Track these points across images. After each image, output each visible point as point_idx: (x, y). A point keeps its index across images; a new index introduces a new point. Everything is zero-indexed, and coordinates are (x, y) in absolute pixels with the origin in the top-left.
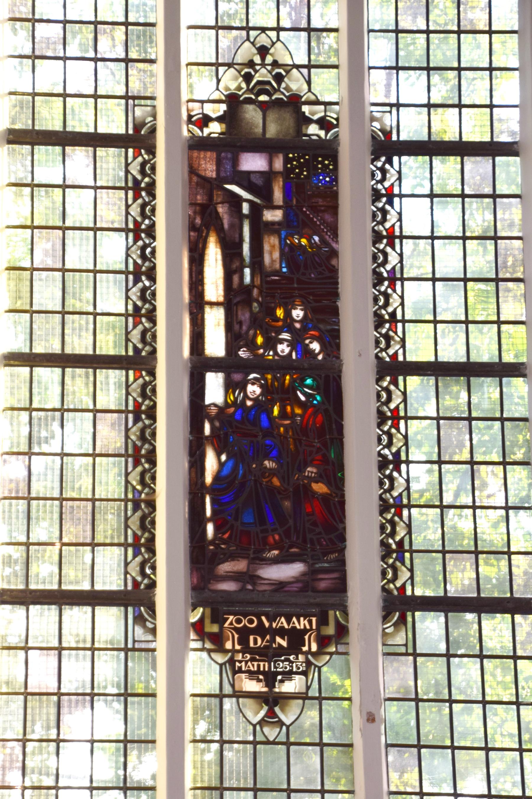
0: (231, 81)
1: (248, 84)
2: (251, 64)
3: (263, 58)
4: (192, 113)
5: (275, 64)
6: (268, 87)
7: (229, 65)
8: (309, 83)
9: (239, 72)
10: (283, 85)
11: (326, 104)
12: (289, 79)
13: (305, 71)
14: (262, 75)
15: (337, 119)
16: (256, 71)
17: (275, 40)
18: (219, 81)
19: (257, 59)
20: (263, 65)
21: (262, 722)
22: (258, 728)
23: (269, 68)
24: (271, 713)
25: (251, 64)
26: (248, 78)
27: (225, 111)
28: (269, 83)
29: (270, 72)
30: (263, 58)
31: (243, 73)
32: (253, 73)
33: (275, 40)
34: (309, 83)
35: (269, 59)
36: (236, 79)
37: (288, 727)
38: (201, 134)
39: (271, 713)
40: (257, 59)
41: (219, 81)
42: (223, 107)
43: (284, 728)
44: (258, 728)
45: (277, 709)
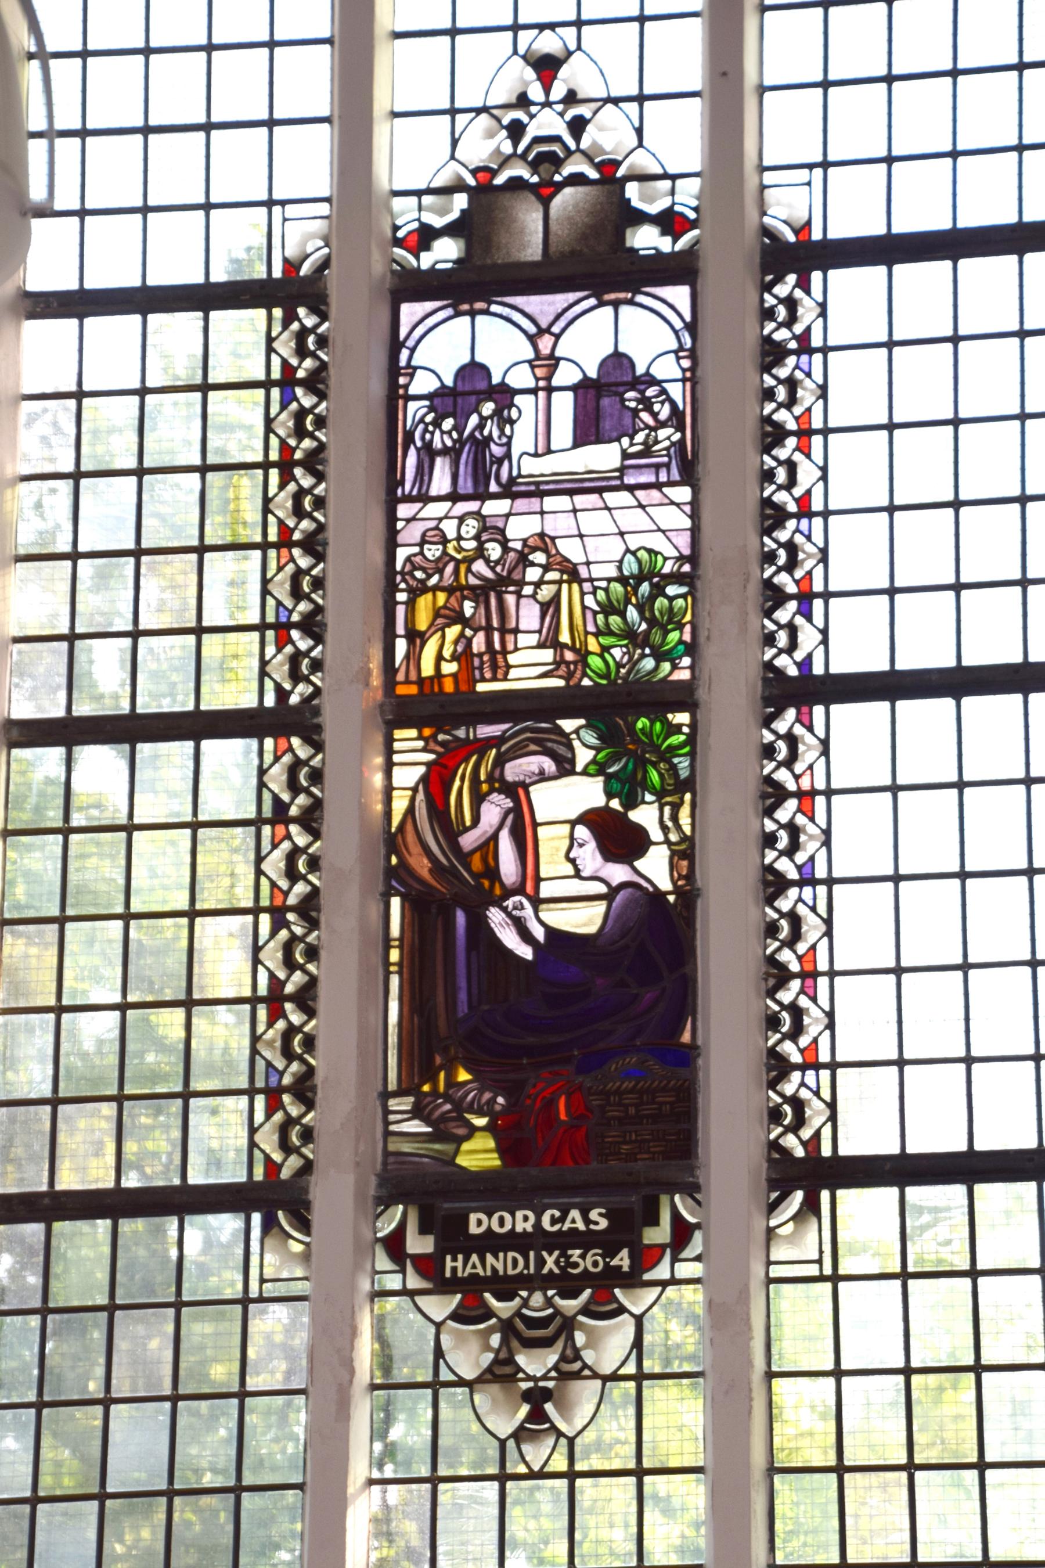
0: (481, 144)
1: (515, 145)
2: (523, 101)
3: (547, 89)
4: (399, 222)
5: (571, 98)
6: (556, 148)
7: (478, 111)
8: (639, 131)
9: (498, 120)
10: (585, 144)
11: (674, 178)
12: (601, 129)
13: (632, 108)
14: (548, 123)
15: (696, 209)
16: (532, 117)
17: (572, 46)
18: (455, 142)
19: (536, 92)
20: (547, 104)
21: (520, 1435)
22: (511, 1444)
23: (559, 107)
24: (537, 1415)
25: (523, 101)
26: (516, 130)
27: (463, 211)
28: (557, 139)
29: (561, 114)
30: (547, 89)
31: (505, 121)
32: (525, 119)
33: (572, 46)
34: (639, 131)
35: (558, 91)
36: (491, 135)
37: (571, 1441)
38: (415, 263)
39: (537, 1415)
40: (536, 92)
41: (455, 142)
42: (461, 201)
43: (563, 1441)
44: (511, 1444)
45: (549, 1407)
